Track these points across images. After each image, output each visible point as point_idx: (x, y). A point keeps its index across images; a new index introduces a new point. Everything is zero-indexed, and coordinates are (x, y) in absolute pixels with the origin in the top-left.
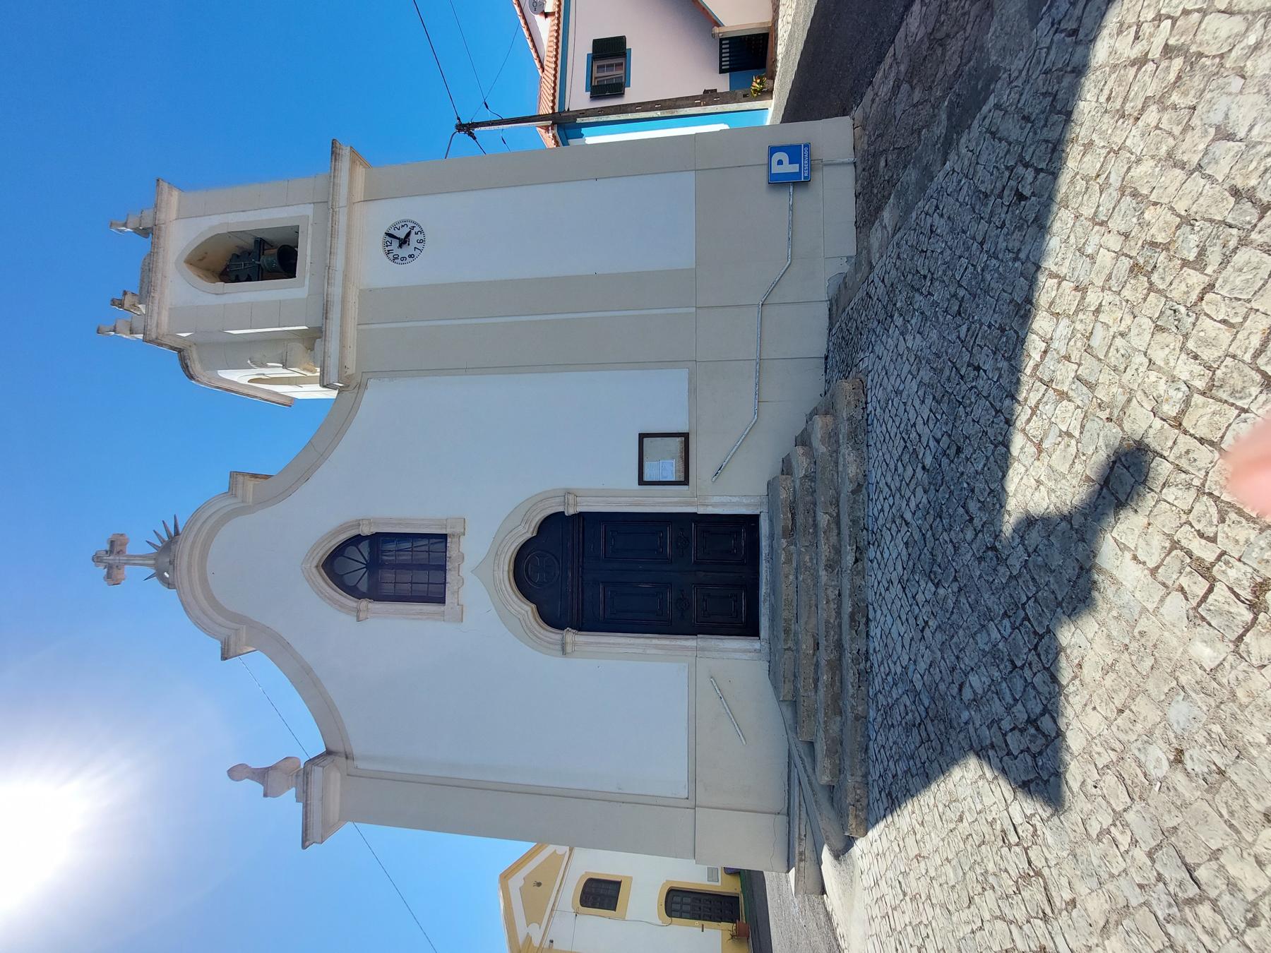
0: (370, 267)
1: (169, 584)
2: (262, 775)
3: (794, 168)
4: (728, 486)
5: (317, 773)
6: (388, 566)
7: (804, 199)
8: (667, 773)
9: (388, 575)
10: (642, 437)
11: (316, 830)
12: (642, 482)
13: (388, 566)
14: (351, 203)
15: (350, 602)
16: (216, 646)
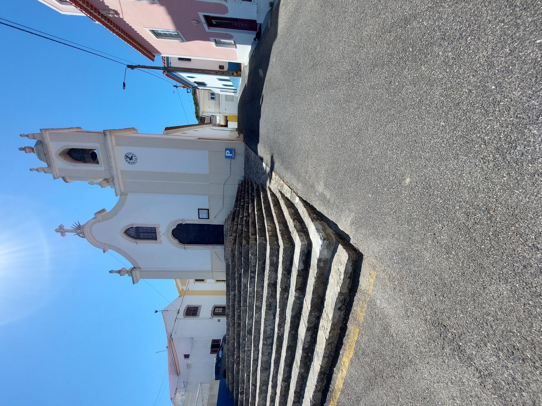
0: (121, 164)
1: (84, 237)
2: (119, 272)
3: (231, 155)
4: (218, 218)
5: (134, 272)
6: (143, 234)
7: (233, 161)
8: (208, 267)
9: (142, 234)
10: (199, 209)
11: (135, 280)
12: (199, 218)
13: (143, 234)
14: (113, 148)
15: (134, 240)
16: (102, 251)
